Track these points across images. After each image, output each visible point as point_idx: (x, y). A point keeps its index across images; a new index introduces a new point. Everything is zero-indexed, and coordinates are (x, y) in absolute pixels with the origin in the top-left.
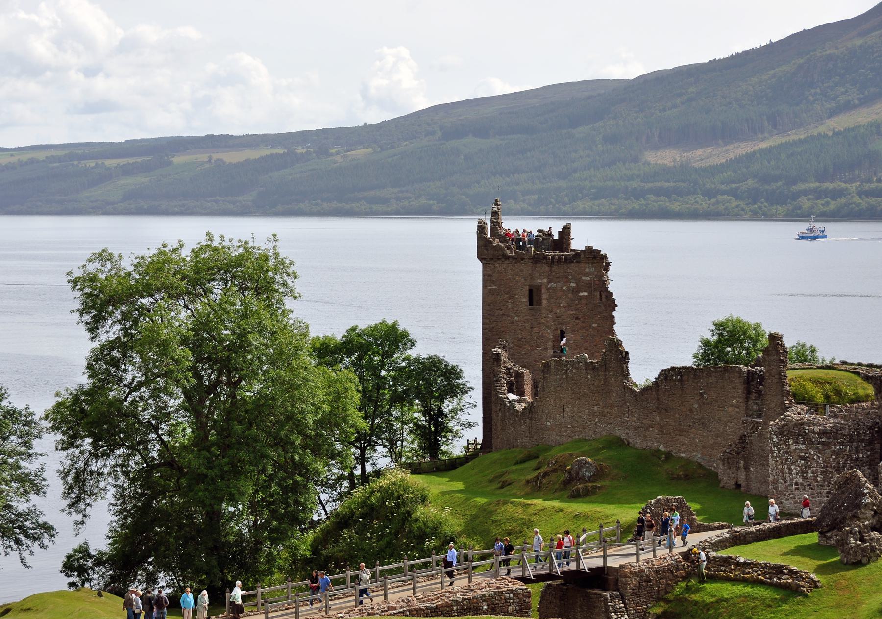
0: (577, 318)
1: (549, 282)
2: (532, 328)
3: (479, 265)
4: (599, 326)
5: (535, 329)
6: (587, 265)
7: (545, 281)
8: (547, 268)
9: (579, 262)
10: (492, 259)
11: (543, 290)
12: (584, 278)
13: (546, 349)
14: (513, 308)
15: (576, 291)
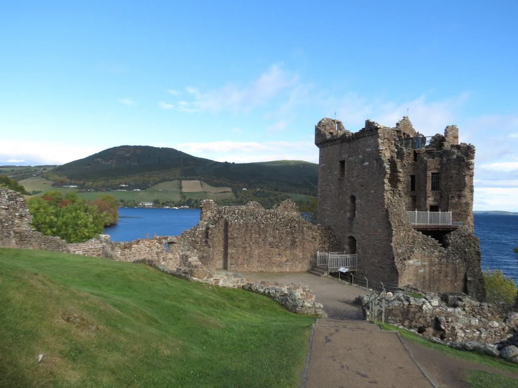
0: (362, 186)
1: (349, 157)
2: (339, 195)
3: (317, 149)
4: (375, 192)
5: (341, 196)
6: (370, 138)
7: (347, 155)
8: (347, 145)
9: (364, 137)
10: (321, 143)
11: (346, 164)
12: (367, 150)
13: (345, 212)
14: (331, 179)
15: (363, 161)
